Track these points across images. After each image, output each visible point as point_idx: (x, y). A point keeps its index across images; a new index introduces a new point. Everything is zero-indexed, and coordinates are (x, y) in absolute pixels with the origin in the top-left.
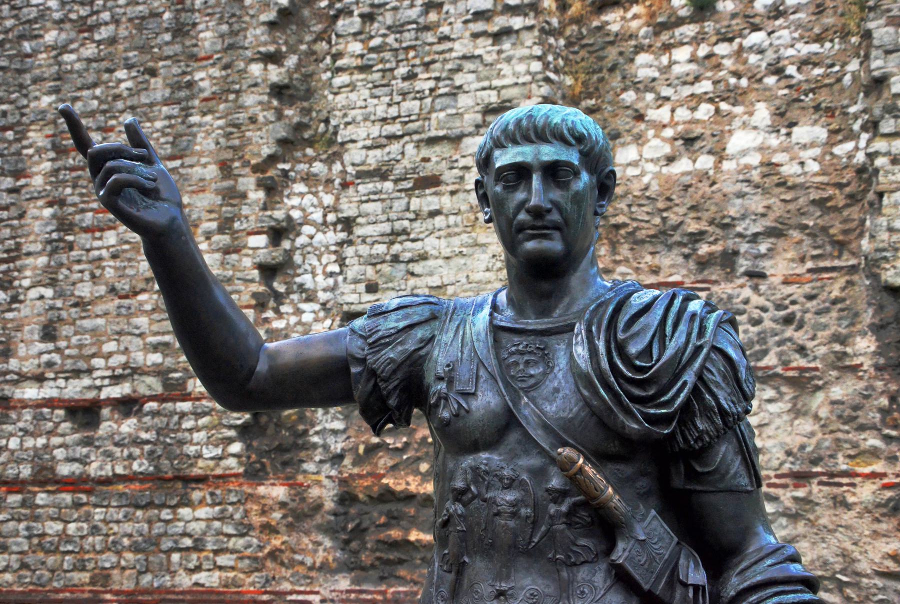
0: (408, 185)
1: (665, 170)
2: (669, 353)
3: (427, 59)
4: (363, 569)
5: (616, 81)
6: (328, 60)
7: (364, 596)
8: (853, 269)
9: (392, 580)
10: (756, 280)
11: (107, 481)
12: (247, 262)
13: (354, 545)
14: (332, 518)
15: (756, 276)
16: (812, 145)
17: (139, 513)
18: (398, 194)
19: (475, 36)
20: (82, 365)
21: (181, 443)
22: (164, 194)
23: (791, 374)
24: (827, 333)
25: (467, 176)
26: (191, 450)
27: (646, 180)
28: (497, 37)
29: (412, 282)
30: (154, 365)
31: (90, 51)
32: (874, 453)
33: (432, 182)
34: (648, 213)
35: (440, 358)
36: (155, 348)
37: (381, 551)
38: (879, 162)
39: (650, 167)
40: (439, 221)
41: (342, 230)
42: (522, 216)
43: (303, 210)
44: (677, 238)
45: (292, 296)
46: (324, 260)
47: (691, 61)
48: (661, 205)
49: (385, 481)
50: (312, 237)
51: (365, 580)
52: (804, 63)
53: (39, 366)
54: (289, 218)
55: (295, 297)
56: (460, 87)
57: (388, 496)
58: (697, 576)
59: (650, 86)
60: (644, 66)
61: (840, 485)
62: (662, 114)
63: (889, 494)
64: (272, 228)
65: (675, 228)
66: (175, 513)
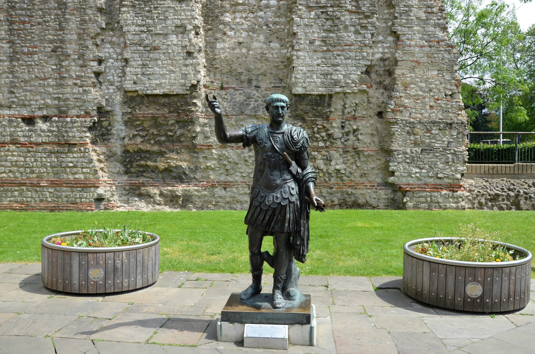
3: (155, 6)
4: (131, 173)
7: (133, 182)
9: (142, 177)
12: (89, 71)
13: (129, 166)
15: (257, 87)
17: (53, 155)
21: (67, 132)
27: (226, 54)
30: (55, 104)
33: (155, 49)
36: (55, 99)
38: (294, 57)
39: (227, 50)
40: (159, 62)
41: (124, 62)
43: (109, 53)
44: (234, 73)
45: (105, 83)
47: (241, 18)
48: (230, 63)
49: (139, 146)
50: (113, 63)
51: (133, 176)
52: (275, 23)
53: (9, 102)
56: (167, 17)
57: (140, 151)
60: (228, 18)
62: (232, 33)
64: (98, 59)
65: (234, 70)
66: (66, 155)
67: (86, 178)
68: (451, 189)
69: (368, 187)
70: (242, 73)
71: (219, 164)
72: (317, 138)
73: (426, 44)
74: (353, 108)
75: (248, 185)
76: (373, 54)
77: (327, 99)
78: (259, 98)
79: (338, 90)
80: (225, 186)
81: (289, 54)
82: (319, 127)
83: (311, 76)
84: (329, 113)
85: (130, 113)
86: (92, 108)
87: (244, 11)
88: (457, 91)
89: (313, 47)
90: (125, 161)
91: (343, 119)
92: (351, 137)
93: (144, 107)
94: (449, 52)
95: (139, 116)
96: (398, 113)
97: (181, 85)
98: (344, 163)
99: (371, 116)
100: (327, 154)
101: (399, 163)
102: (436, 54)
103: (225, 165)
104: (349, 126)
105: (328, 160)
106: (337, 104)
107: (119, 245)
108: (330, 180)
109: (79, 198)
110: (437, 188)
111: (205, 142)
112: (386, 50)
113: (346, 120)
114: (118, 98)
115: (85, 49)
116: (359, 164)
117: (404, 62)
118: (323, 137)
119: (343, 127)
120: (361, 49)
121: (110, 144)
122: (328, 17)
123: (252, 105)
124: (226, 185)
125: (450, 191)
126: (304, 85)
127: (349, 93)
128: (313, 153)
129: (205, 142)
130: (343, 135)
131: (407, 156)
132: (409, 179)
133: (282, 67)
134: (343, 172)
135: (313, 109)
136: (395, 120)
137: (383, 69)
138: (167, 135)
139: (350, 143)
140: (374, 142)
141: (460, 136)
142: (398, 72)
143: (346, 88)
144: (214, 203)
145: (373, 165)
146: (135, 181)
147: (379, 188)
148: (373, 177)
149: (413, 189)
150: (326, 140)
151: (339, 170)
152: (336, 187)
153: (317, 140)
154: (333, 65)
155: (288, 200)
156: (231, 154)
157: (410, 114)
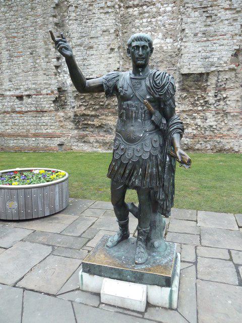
2: (163, 83)
5: (130, 26)
6: (67, 17)
8: (176, 70)
11: (26, 112)
12: (52, 65)
19: (101, 13)
20: (18, 87)
22: (69, 49)
26: (43, 105)
28: (105, 13)
31: (12, 13)
33: (91, 48)
35: (120, 84)
36: (34, 84)
38: (182, 47)
42: (138, 56)
55: (63, 73)
57: (84, 115)
58: (164, 122)
59: (138, 27)
69: (233, 138)
79: (213, 69)
86: (54, 88)
87: (149, 17)
91: (216, 90)
92: (222, 103)
98: (215, 121)
99: (237, 87)
105: (205, 119)
106: (213, 80)
107: (43, 182)
113: (219, 91)
119: (216, 96)
122: (208, 15)
126: (189, 67)
127: (222, 71)
133: (174, 55)
134: (214, 127)
138: (99, 104)
139: (220, 107)
146: (82, 133)
151: (212, 126)
154: (211, 51)
155: (149, 154)
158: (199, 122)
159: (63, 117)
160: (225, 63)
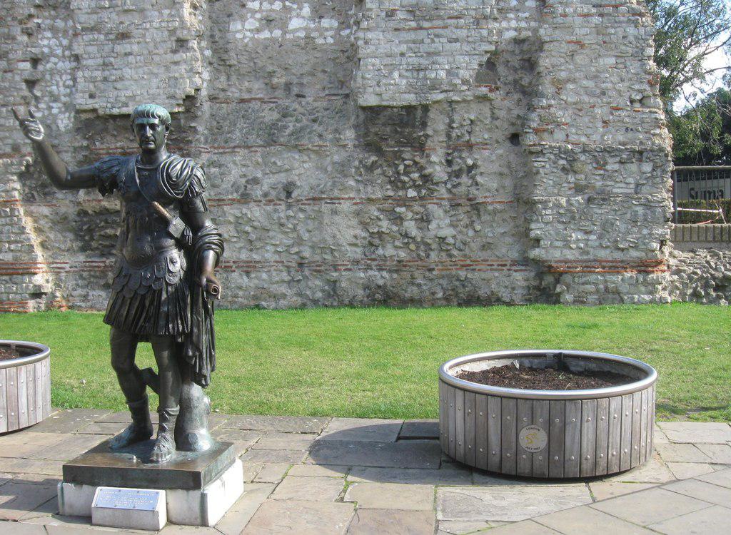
0: (112, 37)
1: (256, 36)
7: (94, 264)
10: (300, 99)
12: (17, 78)
13: (87, 238)
14: (74, 223)
16: (331, 29)
18: (107, 42)
23: (315, 148)
24: (333, 128)
25: (147, 34)
27: (246, 41)
29: (116, 92)
32: (351, 188)
33: (124, 36)
34: (246, 59)
37: (102, 240)
38: (360, 43)
39: (248, 34)
41: (74, 61)
46: (64, 77)
51: (94, 256)
54: (43, 52)
55: (46, 99)
61: (334, 203)
63: (355, 207)
67: (16, 259)
68: (643, 268)
70: (274, 72)
71: (238, 232)
72: (404, 182)
73: (594, 10)
74: (466, 128)
75: (288, 267)
76: (500, 32)
77: (419, 113)
78: (304, 115)
80: (248, 268)
81: (352, 37)
82: (405, 162)
83: (391, 73)
84: (423, 138)
85: (87, 147)
88: (651, 94)
89: (392, 24)
90: (81, 230)
92: (464, 179)
93: (109, 138)
94: (636, 24)
95: (101, 151)
96: (545, 135)
97: (168, 98)
98: (452, 225)
99: (498, 142)
100: (422, 210)
101: (547, 223)
102: (612, 27)
103: (247, 233)
104: (459, 161)
105: (424, 220)
106: (437, 123)
108: (428, 256)
109: (6, 293)
110: (616, 267)
111: (212, 193)
112: (523, 25)
113: (455, 149)
114: (65, 122)
115: (9, 42)
116: (478, 228)
117: (555, 43)
118: (414, 181)
119: (449, 163)
120: (478, 24)
121: (54, 201)
123: (291, 128)
124: (248, 267)
125: (640, 272)
128: (398, 209)
129: (212, 193)
130: (450, 177)
131: (561, 211)
132: (567, 252)
133: (343, 60)
134: (451, 241)
135: (396, 132)
136: (539, 148)
137: (518, 58)
139: (462, 189)
140: (503, 187)
141: (659, 172)
142: (544, 62)
143: (451, 94)
144: (230, 299)
145: (497, 231)
147: (514, 268)
148: (504, 251)
149: (572, 270)
150: (419, 185)
151: (444, 239)
152: (440, 267)
153: (404, 187)
154: (429, 54)
156: (257, 214)
157: (567, 136)
158: (411, 227)
159: (46, 216)
160: (465, 82)
